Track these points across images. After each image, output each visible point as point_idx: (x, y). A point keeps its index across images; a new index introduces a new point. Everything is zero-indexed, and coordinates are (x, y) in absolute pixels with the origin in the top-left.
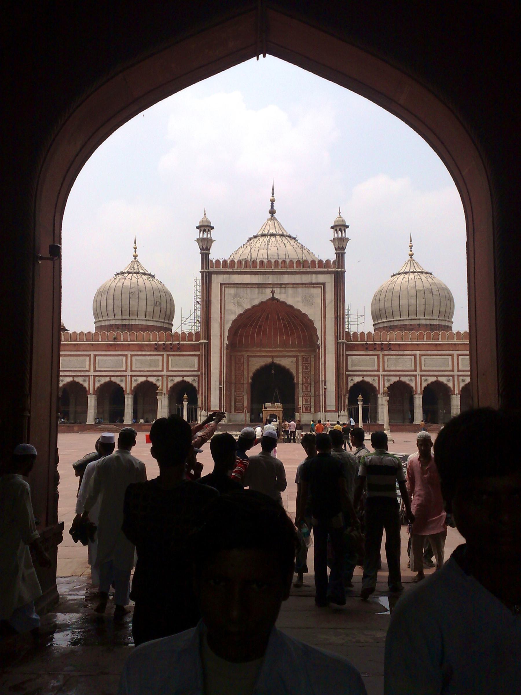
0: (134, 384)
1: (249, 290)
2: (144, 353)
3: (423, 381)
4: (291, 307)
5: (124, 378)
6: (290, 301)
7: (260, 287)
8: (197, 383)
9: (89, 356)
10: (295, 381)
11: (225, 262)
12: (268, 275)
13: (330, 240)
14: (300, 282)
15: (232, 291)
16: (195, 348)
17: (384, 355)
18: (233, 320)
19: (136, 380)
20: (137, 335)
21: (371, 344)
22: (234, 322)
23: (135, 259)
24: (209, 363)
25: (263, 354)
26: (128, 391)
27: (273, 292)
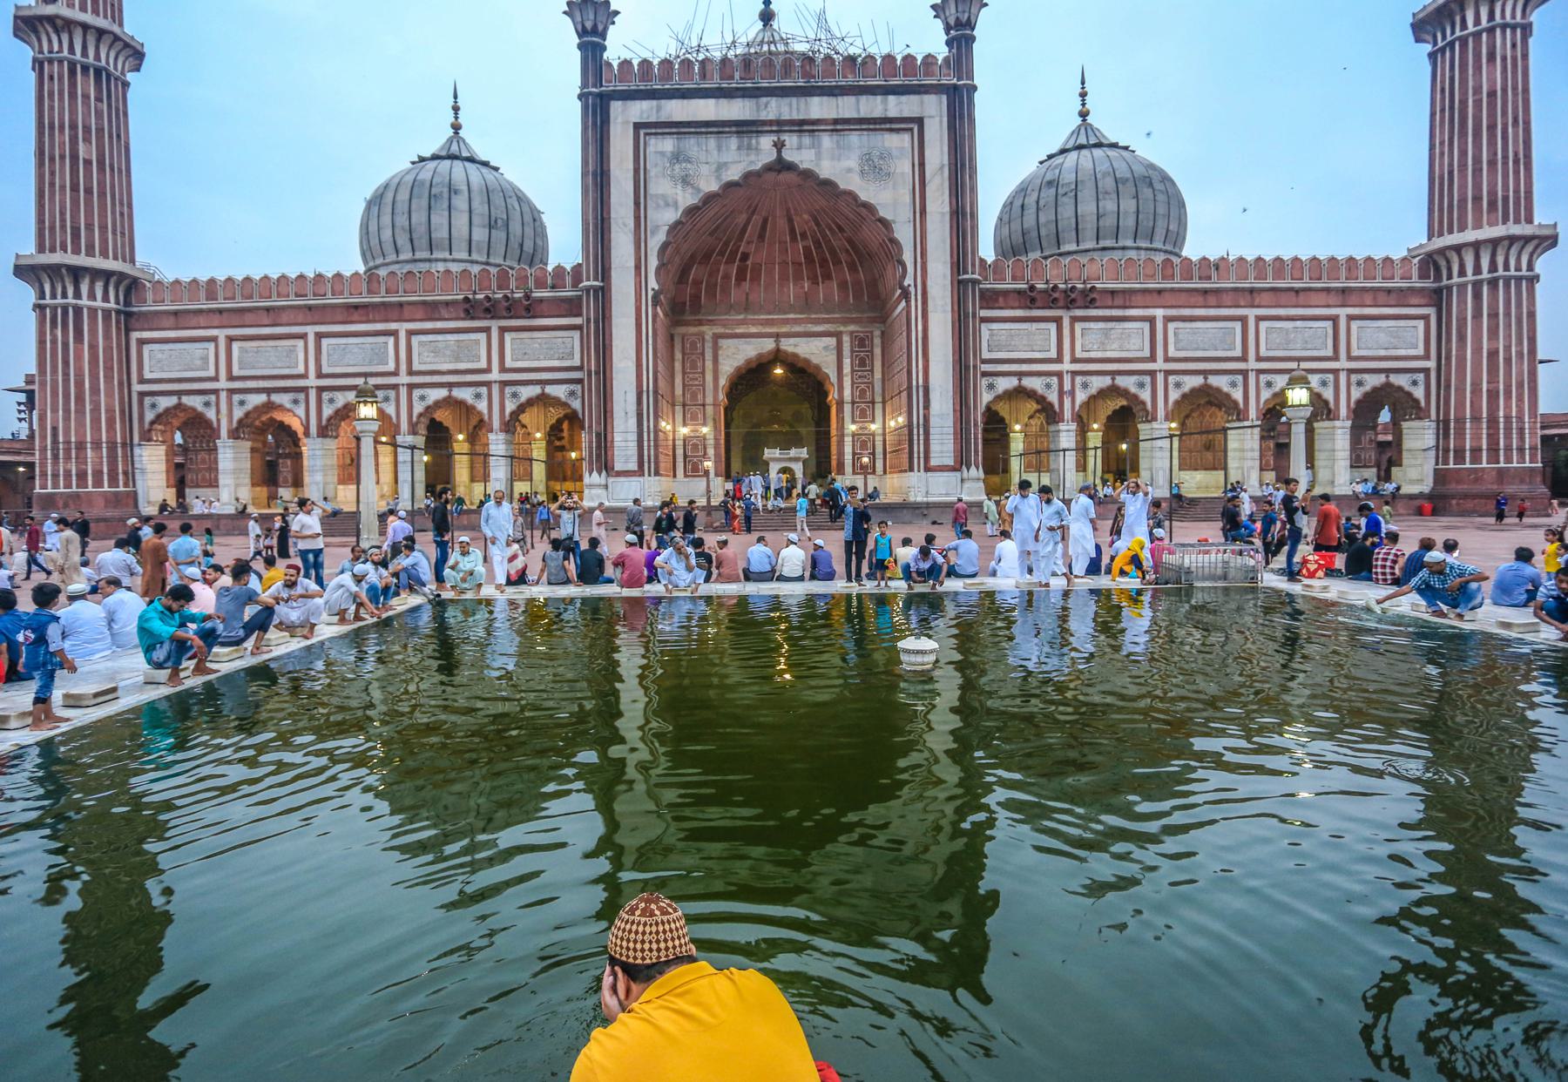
1: (712, 142)
2: (439, 325)
3: (1171, 387)
4: (829, 184)
6: (826, 170)
7: (743, 132)
8: (579, 400)
9: (303, 336)
11: (645, 63)
12: (764, 100)
14: (855, 115)
15: (668, 145)
17: (1074, 319)
18: (671, 222)
21: (1045, 291)
22: (675, 227)
23: (456, 133)
24: (607, 342)
27: (779, 146)
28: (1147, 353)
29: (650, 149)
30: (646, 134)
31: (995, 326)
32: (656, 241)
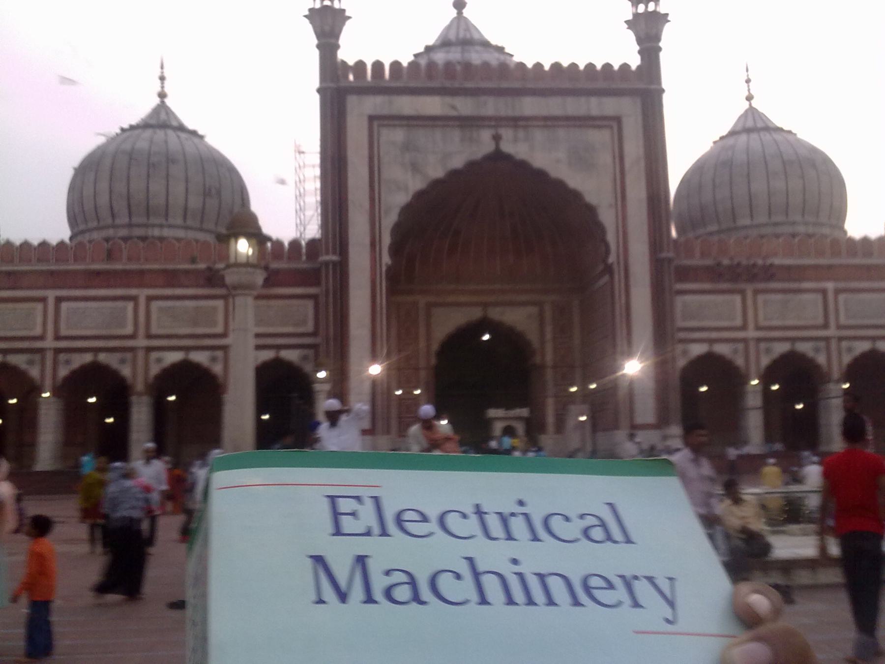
0: (155, 370)
1: (438, 134)
4: (541, 175)
5: (129, 356)
9: (43, 300)
10: (538, 359)
12: (483, 98)
13: (626, 22)
15: (397, 135)
16: (310, 277)
17: (756, 292)
19: (159, 360)
20: (161, 248)
25: (463, 299)
26: (140, 386)
27: (497, 138)
28: (820, 321)
29: (383, 139)
30: (379, 126)
31: (688, 298)
32: (390, 220)
